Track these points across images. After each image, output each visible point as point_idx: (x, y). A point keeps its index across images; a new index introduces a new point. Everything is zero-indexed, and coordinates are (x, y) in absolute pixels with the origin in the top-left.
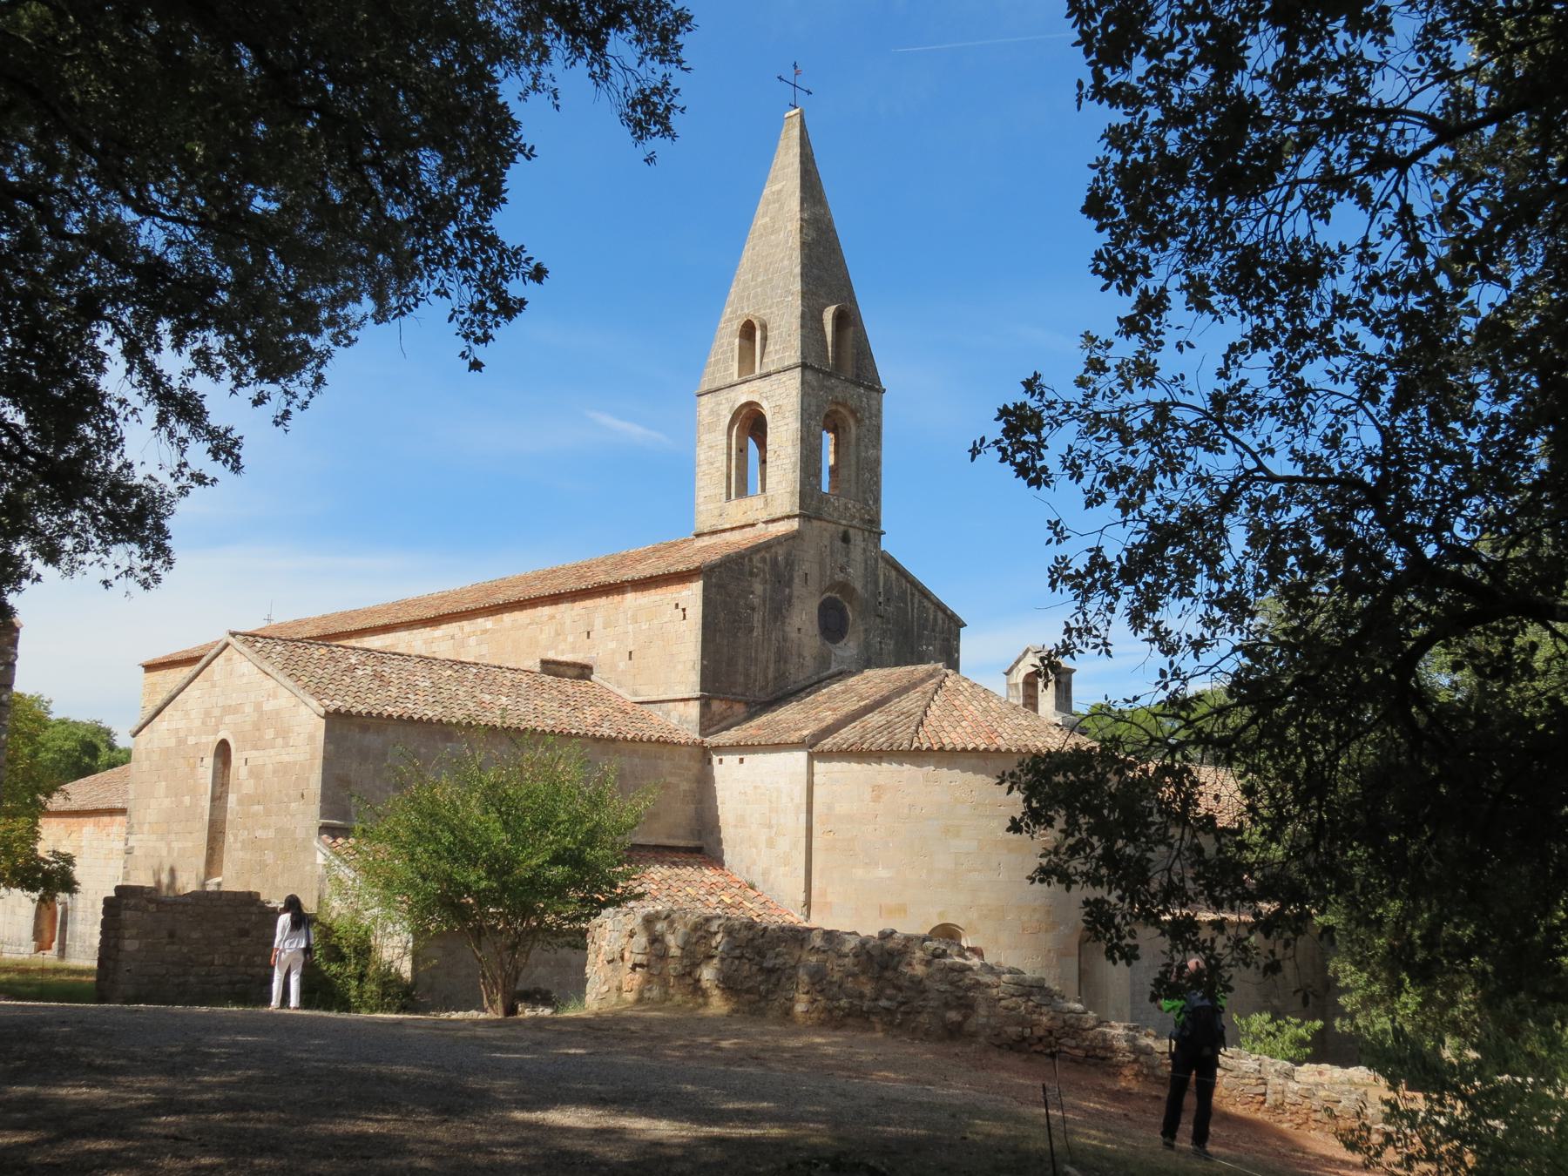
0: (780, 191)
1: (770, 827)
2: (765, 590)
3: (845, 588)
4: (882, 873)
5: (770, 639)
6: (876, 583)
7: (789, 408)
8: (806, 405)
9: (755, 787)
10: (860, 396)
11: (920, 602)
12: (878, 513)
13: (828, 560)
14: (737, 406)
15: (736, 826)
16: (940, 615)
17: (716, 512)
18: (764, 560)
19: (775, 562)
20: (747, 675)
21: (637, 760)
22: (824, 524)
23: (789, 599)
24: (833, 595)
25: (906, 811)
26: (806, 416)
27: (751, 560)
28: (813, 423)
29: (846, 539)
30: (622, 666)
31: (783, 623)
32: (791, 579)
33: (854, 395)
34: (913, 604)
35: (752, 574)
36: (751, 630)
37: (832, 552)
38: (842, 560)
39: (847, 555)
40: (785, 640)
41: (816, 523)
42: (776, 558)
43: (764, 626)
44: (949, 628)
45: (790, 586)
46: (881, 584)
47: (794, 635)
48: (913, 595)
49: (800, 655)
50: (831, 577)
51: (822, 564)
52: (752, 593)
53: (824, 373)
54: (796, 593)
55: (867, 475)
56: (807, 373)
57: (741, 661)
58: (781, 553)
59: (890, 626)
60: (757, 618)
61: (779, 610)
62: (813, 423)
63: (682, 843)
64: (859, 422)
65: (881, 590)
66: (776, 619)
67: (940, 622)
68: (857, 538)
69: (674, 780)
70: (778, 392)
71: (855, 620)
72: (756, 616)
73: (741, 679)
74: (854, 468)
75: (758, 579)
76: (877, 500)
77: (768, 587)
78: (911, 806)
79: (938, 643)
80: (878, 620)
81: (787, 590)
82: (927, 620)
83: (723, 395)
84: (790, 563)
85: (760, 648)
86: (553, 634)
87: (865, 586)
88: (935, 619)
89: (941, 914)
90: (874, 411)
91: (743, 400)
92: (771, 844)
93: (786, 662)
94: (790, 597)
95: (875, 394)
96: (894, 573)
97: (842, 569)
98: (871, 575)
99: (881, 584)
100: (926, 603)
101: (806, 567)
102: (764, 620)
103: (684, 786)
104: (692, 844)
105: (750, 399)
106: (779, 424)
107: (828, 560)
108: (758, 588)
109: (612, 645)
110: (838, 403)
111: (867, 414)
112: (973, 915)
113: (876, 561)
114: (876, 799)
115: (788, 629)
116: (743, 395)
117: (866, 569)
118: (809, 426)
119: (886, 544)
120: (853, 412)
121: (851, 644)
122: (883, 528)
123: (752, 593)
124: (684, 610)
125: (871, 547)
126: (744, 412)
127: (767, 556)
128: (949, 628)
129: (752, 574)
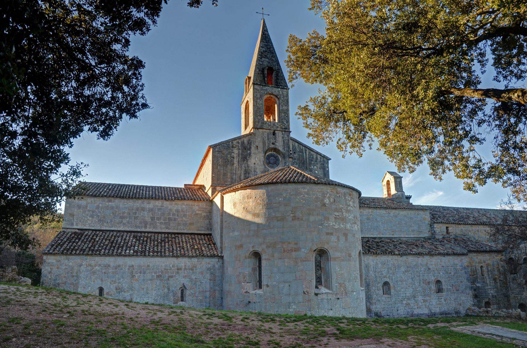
2: (239, 152)
4: (236, 233)
5: (241, 167)
6: (289, 147)
8: (255, 95)
10: (279, 91)
11: (309, 152)
12: (289, 126)
13: (267, 141)
16: (319, 156)
18: (238, 143)
19: (243, 143)
20: (232, 178)
21: (184, 206)
22: (264, 130)
23: (250, 154)
24: (272, 153)
26: (255, 98)
27: (232, 143)
28: (258, 100)
29: (274, 134)
31: (247, 161)
33: (276, 91)
34: (306, 153)
35: (233, 147)
36: (233, 164)
37: (268, 139)
38: (273, 141)
39: (275, 139)
40: (248, 167)
41: (261, 130)
43: (239, 163)
44: (324, 160)
47: (253, 165)
48: (306, 150)
50: (268, 146)
51: (264, 143)
54: (252, 152)
55: (283, 114)
56: (255, 86)
57: (229, 174)
58: (246, 140)
60: (236, 161)
61: (245, 157)
62: (258, 100)
63: (203, 232)
64: (278, 99)
65: (291, 149)
66: (244, 161)
67: (319, 158)
68: (279, 134)
69: (200, 212)
72: (235, 160)
73: (230, 180)
76: (288, 122)
77: (240, 151)
79: (319, 166)
80: (291, 159)
81: (249, 152)
82: (313, 158)
84: (249, 143)
85: (237, 170)
87: (284, 149)
88: (317, 158)
89: (253, 247)
90: (285, 95)
93: (249, 174)
94: (250, 154)
95: (285, 90)
96: (297, 144)
97: (273, 144)
98: (286, 144)
100: (312, 153)
101: (257, 144)
102: (239, 161)
103: (204, 214)
104: (206, 232)
107: (267, 141)
110: (270, 94)
111: (282, 96)
112: (264, 246)
113: (288, 140)
115: (249, 163)
117: (284, 143)
118: (257, 101)
119: (292, 135)
120: (276, 96)
122: (290, 130)
125: (286, 136)
127: (240, 141)
128: (324, 160)
129: (233, 147)
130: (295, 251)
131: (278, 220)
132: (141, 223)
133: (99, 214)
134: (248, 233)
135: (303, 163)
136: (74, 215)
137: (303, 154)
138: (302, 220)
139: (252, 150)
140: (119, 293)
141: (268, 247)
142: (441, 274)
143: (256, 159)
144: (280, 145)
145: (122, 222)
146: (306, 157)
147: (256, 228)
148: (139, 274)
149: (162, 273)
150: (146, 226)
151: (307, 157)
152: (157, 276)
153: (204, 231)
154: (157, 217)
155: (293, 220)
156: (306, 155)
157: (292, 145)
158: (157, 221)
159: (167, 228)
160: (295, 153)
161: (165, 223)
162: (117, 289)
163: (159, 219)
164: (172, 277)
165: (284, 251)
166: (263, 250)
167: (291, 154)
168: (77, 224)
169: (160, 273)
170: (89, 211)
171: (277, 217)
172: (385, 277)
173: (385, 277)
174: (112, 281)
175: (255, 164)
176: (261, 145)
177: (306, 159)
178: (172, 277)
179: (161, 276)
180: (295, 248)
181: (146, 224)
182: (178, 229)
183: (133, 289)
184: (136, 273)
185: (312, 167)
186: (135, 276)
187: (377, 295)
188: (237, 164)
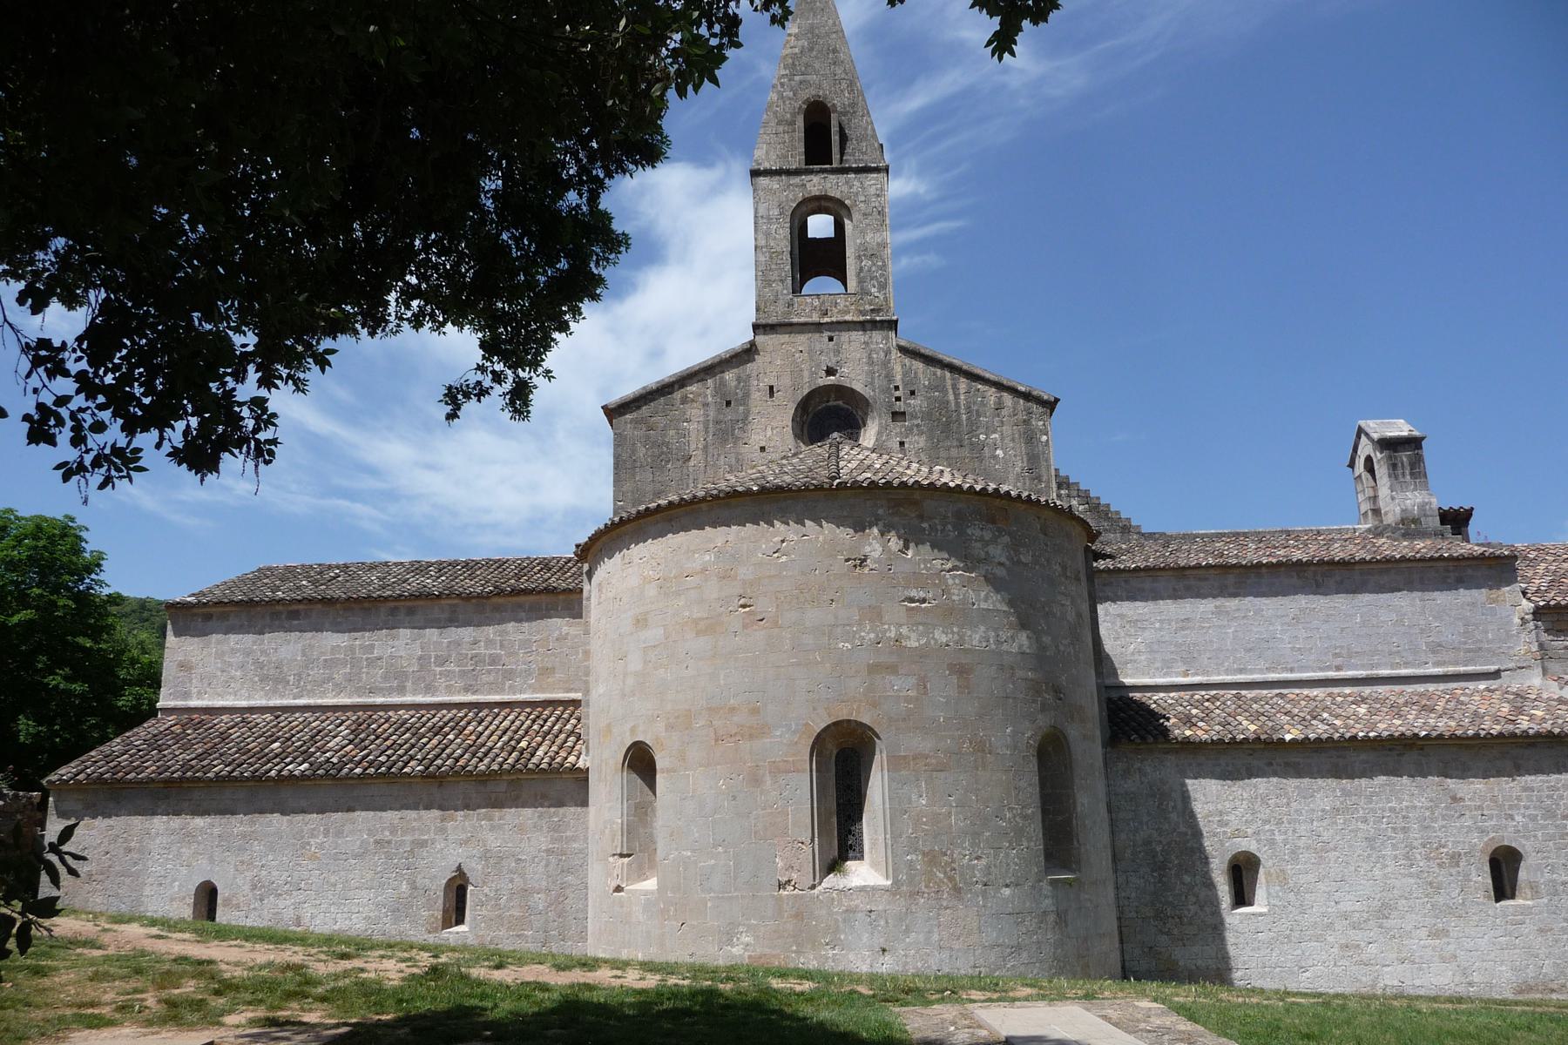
3: (841, 391)
6: (889, 377)
16: (1007, 398)
32: (747, 395)
38: (827, 360)
39: (837, 352)
53: (789, 173)
66: (724, 441)
82: (983, 404)
89: (633, 730)
96: (919, 366)
112: (660, 726)
113: (888, 352)
130: (751, 737)
131: (698, 633)
132: (385, 678)
135: (947, 429)
136: (191, 668)
137: (946, 393)
138: (776, 624)
139: (752, 403)
140: (261, 900)
141: (670, 727)
142: (1518, 818)
143: (769, 433)
144: (855, 377)
148: (320, 839)
149: (391, 833)
150: (404, 687)
152: (376, 842)
154: (437, 657)
155: (745, 626)
156: (957, 396)
158: (438, 669)
160: (913, 393)
161: (463, 674)
162: (254, 887)
163: (440, 661)
164: (423, 844)
165: (716, 740)
166: (657, 739)
167: (898, 399)
168: (199, 693)
169: (387, 833)
171: (696, 622)
172: (1238, 833)
173: (1238, 833)
174: (242, 862)
175: (763, 449)
178: (423, 844)
179: (389, 842)
180: (751, 727)
181: (401, 676)
182: (502, 691)
183: (302, 886)
184: (313, 836)
185: (982, 437)
186: (308, 843)
187: (1201, 907)
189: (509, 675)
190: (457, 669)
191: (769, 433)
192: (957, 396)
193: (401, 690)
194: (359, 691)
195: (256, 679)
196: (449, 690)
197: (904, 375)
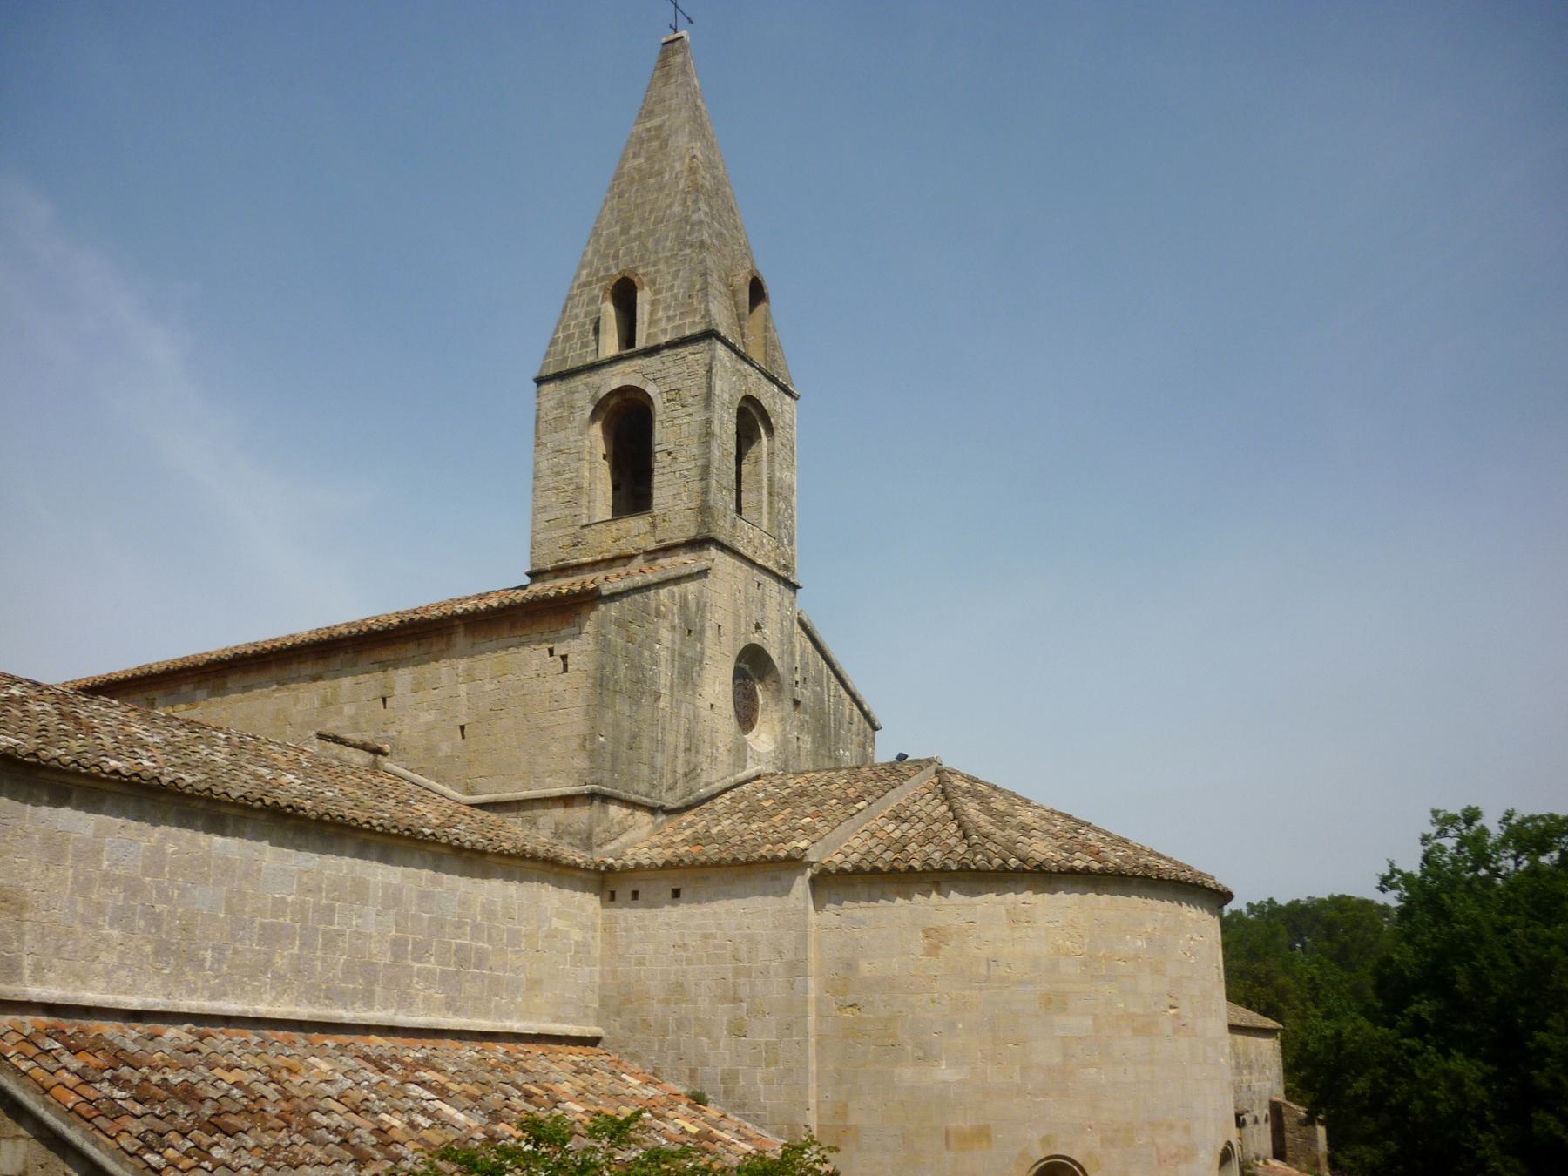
0: (660, 127)
1: (736, 1000)
2: (673, 637)
6: (792, 654)
7: (694, 392)
9: (705, 937)
14: (603, 392)
15: (667, 1002)
17: (567, 541)
25: (983, 970)
30: (445, 749)
32: (702, 631)
34: (829, 690)
40: (696, 717)
42: (686, 596)
43: (672, 695)
45: (701, 640)
46: (798, 658)
47: (705, 713)
49: (713, 744)
52: (659, 642)
54: (708, 652)
55: (782, 504)
59: (807, 717)
67: (856, 719)
70: (673, 370)
71: (767, 704)
74: (765, 491)
75: (666, 623)
77: (677, 636)
78: (992, 962)
83: (579, 382)
86: (317, 703)
91: (615, 383)
92: (738, 1030)
94: (702, 653)
99: (798, 658)
105: (627, 382)
106: (676, 414)
108: (665, 634)
109: (426, 717)
114: (933, 951)
115: (699, 702)
116: (614, 379)
121: (763, 737)
123: (659, 642)
124: (564, 658)
126: (613, 402)
132: (349, 974)
133: (160, 908)
134: (1017, 1078)
136: (22, 907)
137: (822, 688)
145: (269, 963)
146: (829, 706)
147: (1057, 1059)
151: (832, 707)
153: (574, 1021)
157: (801, 645)
158: (416, 965)
159: (451, 1006)
168: (37, 968)
170: (108, 880)
176: (728, 627)
177: (829, 714)
181: (366, 975)
188: (668, 698)
189: (495, 986)
190: (438, 969)
191: (717, 689)
192: (829, 696)
193: (368, 999)
194: (311, 994)
195: (148, 949)
196: (429, 1007)
197: (802, 656)
